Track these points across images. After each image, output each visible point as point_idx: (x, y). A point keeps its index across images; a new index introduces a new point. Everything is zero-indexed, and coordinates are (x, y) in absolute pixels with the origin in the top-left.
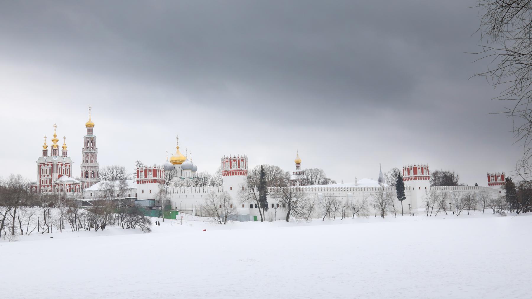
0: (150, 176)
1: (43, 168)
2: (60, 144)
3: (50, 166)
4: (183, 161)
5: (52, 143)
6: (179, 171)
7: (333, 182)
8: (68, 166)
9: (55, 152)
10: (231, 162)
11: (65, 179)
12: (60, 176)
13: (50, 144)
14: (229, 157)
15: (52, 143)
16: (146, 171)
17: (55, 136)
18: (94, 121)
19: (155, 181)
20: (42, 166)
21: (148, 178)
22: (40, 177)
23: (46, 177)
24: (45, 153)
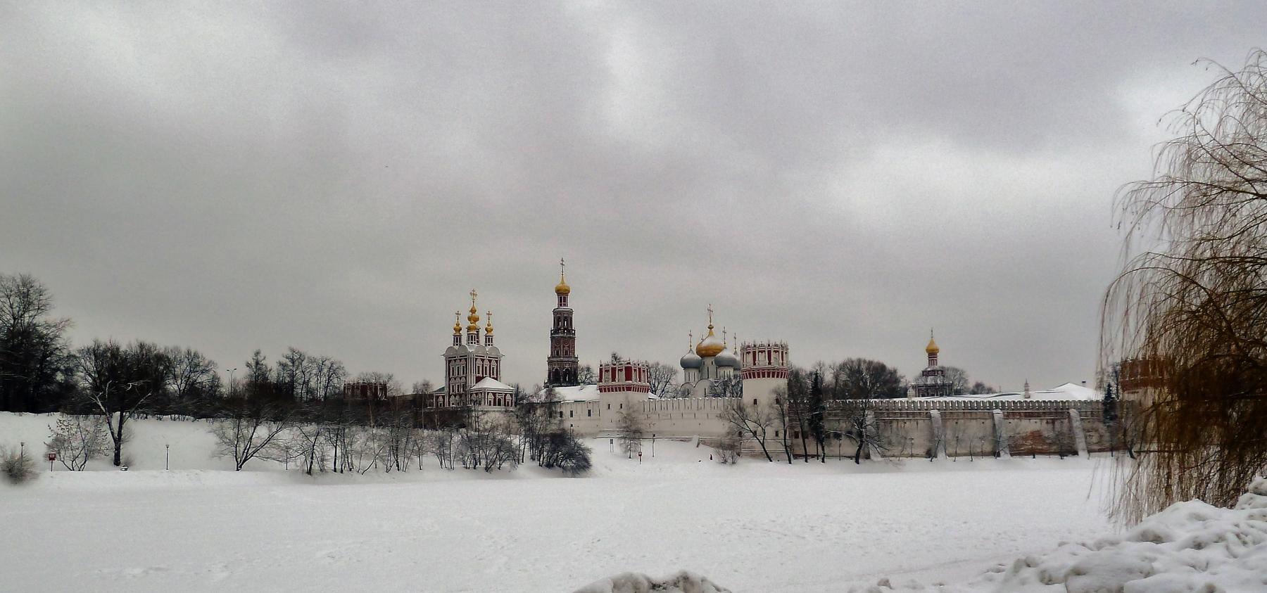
0: (621, 378)
1: (456, 362)
2: (482, 325)
4: (721, 350)
5: (469, 324)
6: (712, 369)
7: (990, 391)
8: (493, 363)
9: (473, 338)
11: (489, 384)
12: (478, 379)
13: (465, 324)
14: (752, 344)
15: (469, 324)
16: (614, 370)
17: (473, 311)
19: (629, 389)
21: (616, 383)
24: (457, 339)
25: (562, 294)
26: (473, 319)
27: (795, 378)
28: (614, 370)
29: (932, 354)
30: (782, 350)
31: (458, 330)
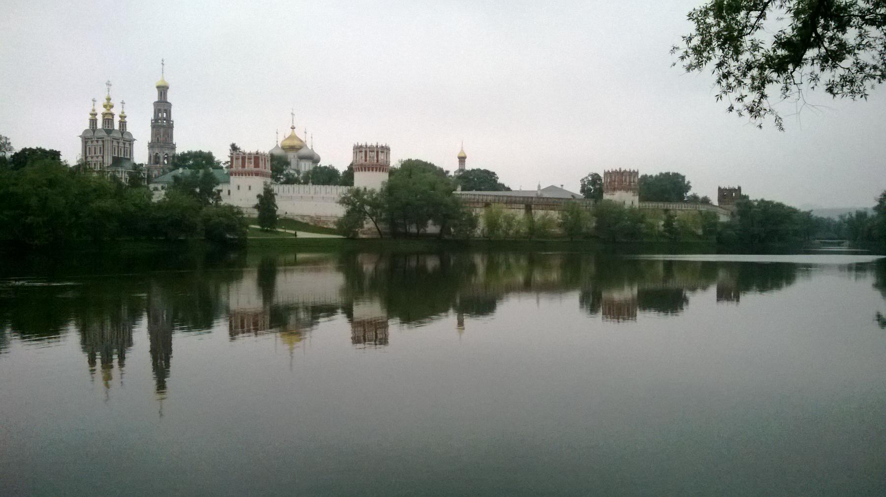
0: (250, 166)
2: (116, 111)
3: (100, 143)
8: (127, 145)
10: (366, 152)
13: (100, 110)
14: (364, 144)
15: (104, 110)
17: (109, 99)
18: (169, 81)
19: (257, 174)
20: (89, 143)
22: (86, 158)
23: (95, 159)
24: (93, 122)
25: (163, 90)
26: (108, 105)
27: (392, 172)
28: (243, 159)
29: (462, 159)
30: (386, 150)
31: (94, 115)
